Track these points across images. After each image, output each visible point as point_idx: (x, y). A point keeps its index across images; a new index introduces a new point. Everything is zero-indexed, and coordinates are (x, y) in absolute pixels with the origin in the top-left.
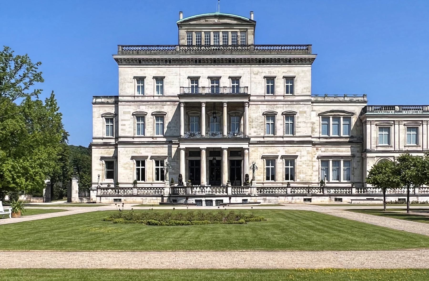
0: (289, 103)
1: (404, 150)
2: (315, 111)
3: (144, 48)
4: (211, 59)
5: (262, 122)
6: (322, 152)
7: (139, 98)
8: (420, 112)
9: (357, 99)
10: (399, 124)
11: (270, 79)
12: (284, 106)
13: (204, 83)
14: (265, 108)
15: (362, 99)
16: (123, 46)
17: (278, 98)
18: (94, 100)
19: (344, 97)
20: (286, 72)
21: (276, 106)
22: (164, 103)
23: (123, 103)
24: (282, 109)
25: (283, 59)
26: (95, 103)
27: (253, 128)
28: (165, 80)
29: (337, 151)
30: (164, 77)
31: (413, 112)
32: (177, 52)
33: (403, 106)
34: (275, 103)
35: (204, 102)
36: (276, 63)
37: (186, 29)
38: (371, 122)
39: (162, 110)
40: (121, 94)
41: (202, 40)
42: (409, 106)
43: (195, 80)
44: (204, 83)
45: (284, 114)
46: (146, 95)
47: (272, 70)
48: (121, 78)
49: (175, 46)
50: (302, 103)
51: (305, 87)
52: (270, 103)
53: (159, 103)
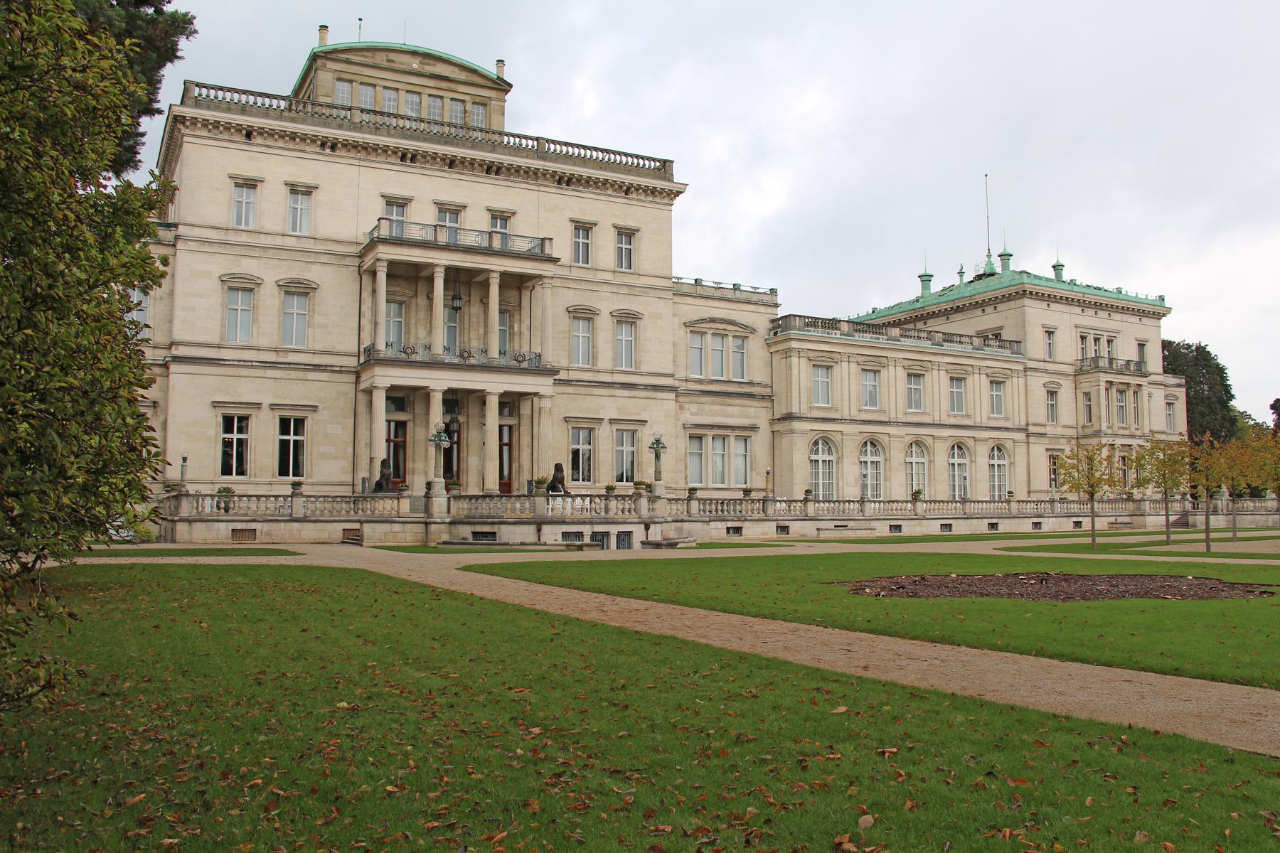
0: (625, 290)
7: (241, 236)
11: (583, 228)
12: (615, 296)
21: (596, 294)
22: (312, 258)
29: (723, 415)
39: (307, 276)
40: (189, 220)
43: (397, 203)
44: (422, 216)
50: (652, 293)
53: (298, 256)
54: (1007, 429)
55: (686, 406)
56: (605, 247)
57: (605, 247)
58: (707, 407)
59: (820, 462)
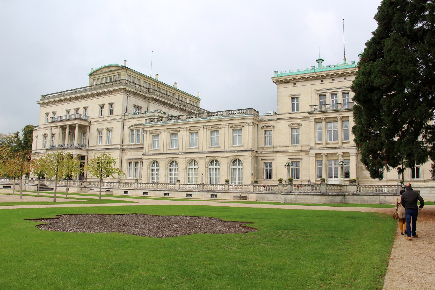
0: (110, 121)
6: (128, 155)
11: (102, 106)
12: (107, 123)
13: (72, 112)
17: (105, 119)
21: (103, 124)
44: (72, 112)
50: (116, 121)
54: (242, 151)
55: (127, 153)
58: (133, 153)
59: (174, 169)
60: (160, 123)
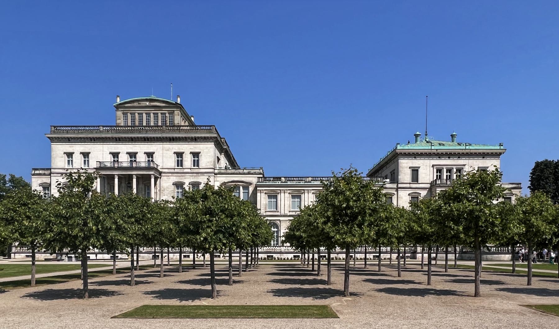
0: (195, 175)
1: (288, 215)
2: (218, 181)
3: (73, 128)
4: (128, 138)
5: (172, 191)
8: (302, 183)
9: (254, 171)
10: (284, 193)
11: (180, 155)
12: (191, 177)
14: (175, 179)
15: (258, 171)
16: (55, 127)
17: (186, 171)
18: (33, 172)
19: (243, 170)
20: (192, 149)
21: (184, 177)
23: (55, 175)
24: (189, 180)
25: (189, 138)
26: (34, 175)
27: (164, 195)
28: (90, 155)
30: (89, 153)
31: (296, 183)
32: (101, 132)
33: (288, 177)
34: (183, 175)
35: (116, 175)
36: (175, 141)
37: (122, 111)
38: (260, 191)
41: (136, 120)
42: (294, 178)
43: (115, 155)
45: (191, 184)
46: (74, 168)
47: (180, 147)
48: (53, 153)
49: (99, 126)
51: (209, 161)
52: (179, 175)
56: (188, 161)
57: (188, 161)
60: (277, 183)
